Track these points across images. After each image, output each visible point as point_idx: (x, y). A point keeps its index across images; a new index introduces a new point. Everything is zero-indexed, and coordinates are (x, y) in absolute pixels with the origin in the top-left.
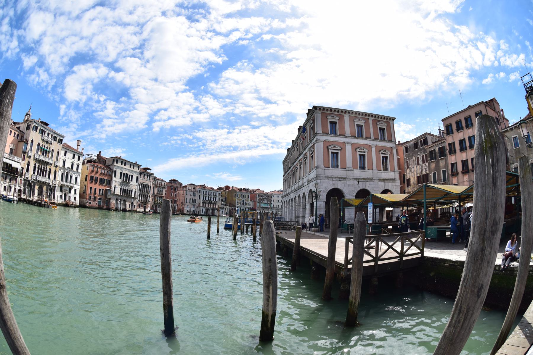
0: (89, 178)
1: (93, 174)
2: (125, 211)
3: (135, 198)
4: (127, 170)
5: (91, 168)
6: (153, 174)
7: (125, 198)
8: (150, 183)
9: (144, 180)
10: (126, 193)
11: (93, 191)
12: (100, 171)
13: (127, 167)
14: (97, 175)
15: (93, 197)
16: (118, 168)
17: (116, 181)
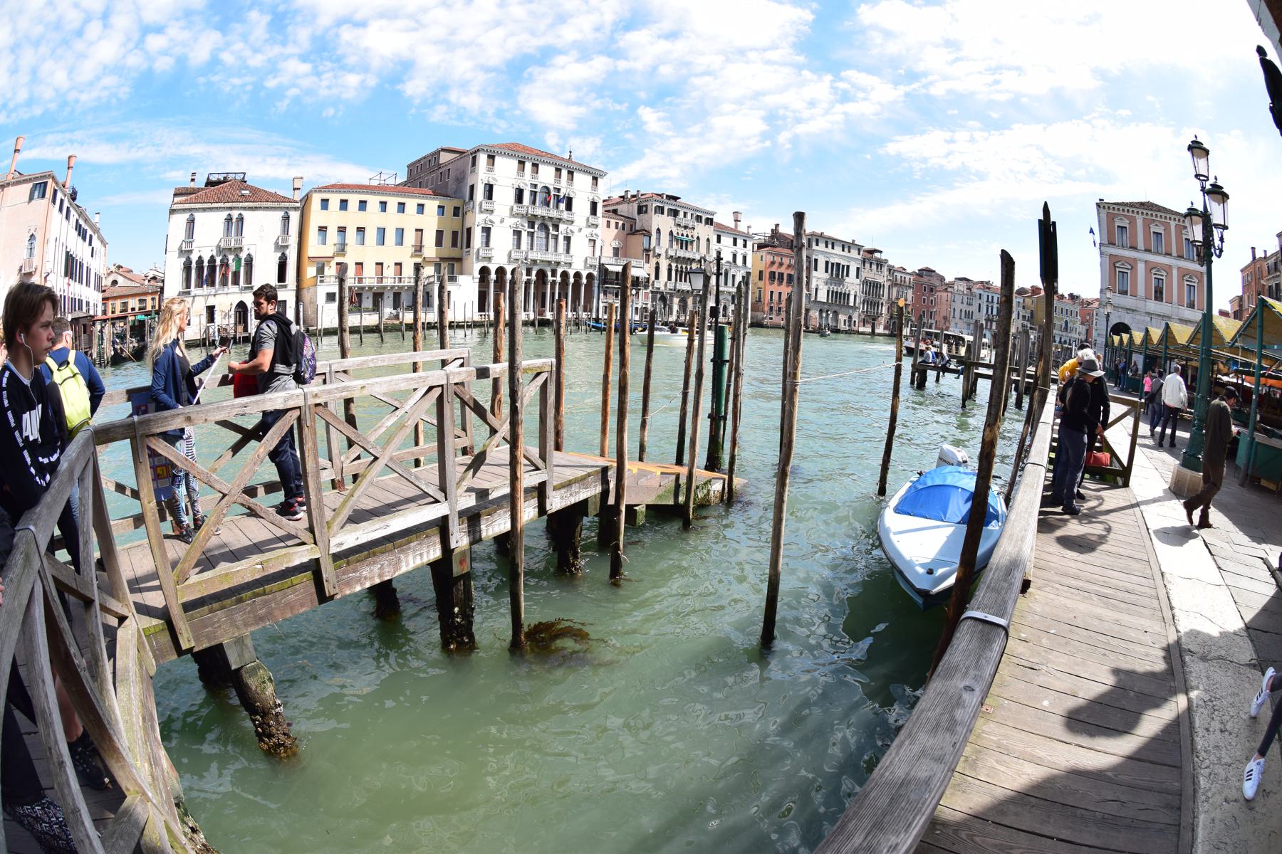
0: (766, 275)
1: (774, 268)
2: (836, 331)
3: (855, 308)
4: (837, 255)
5: (770, 258)
6: (886, 261)
7: (836, 308)
8: (882, 278)
9: (871, 274)
10: (839, 299)
11: (775, 297)
12: (786, 261)
13: (838, 250)
14: (782, 270)
15: (775, 308)
16: (821, 254)
17: (819, 279)
